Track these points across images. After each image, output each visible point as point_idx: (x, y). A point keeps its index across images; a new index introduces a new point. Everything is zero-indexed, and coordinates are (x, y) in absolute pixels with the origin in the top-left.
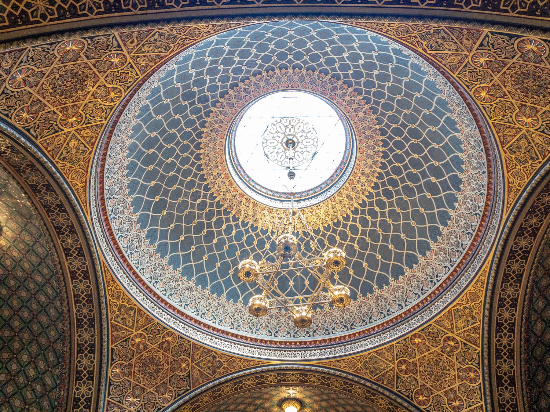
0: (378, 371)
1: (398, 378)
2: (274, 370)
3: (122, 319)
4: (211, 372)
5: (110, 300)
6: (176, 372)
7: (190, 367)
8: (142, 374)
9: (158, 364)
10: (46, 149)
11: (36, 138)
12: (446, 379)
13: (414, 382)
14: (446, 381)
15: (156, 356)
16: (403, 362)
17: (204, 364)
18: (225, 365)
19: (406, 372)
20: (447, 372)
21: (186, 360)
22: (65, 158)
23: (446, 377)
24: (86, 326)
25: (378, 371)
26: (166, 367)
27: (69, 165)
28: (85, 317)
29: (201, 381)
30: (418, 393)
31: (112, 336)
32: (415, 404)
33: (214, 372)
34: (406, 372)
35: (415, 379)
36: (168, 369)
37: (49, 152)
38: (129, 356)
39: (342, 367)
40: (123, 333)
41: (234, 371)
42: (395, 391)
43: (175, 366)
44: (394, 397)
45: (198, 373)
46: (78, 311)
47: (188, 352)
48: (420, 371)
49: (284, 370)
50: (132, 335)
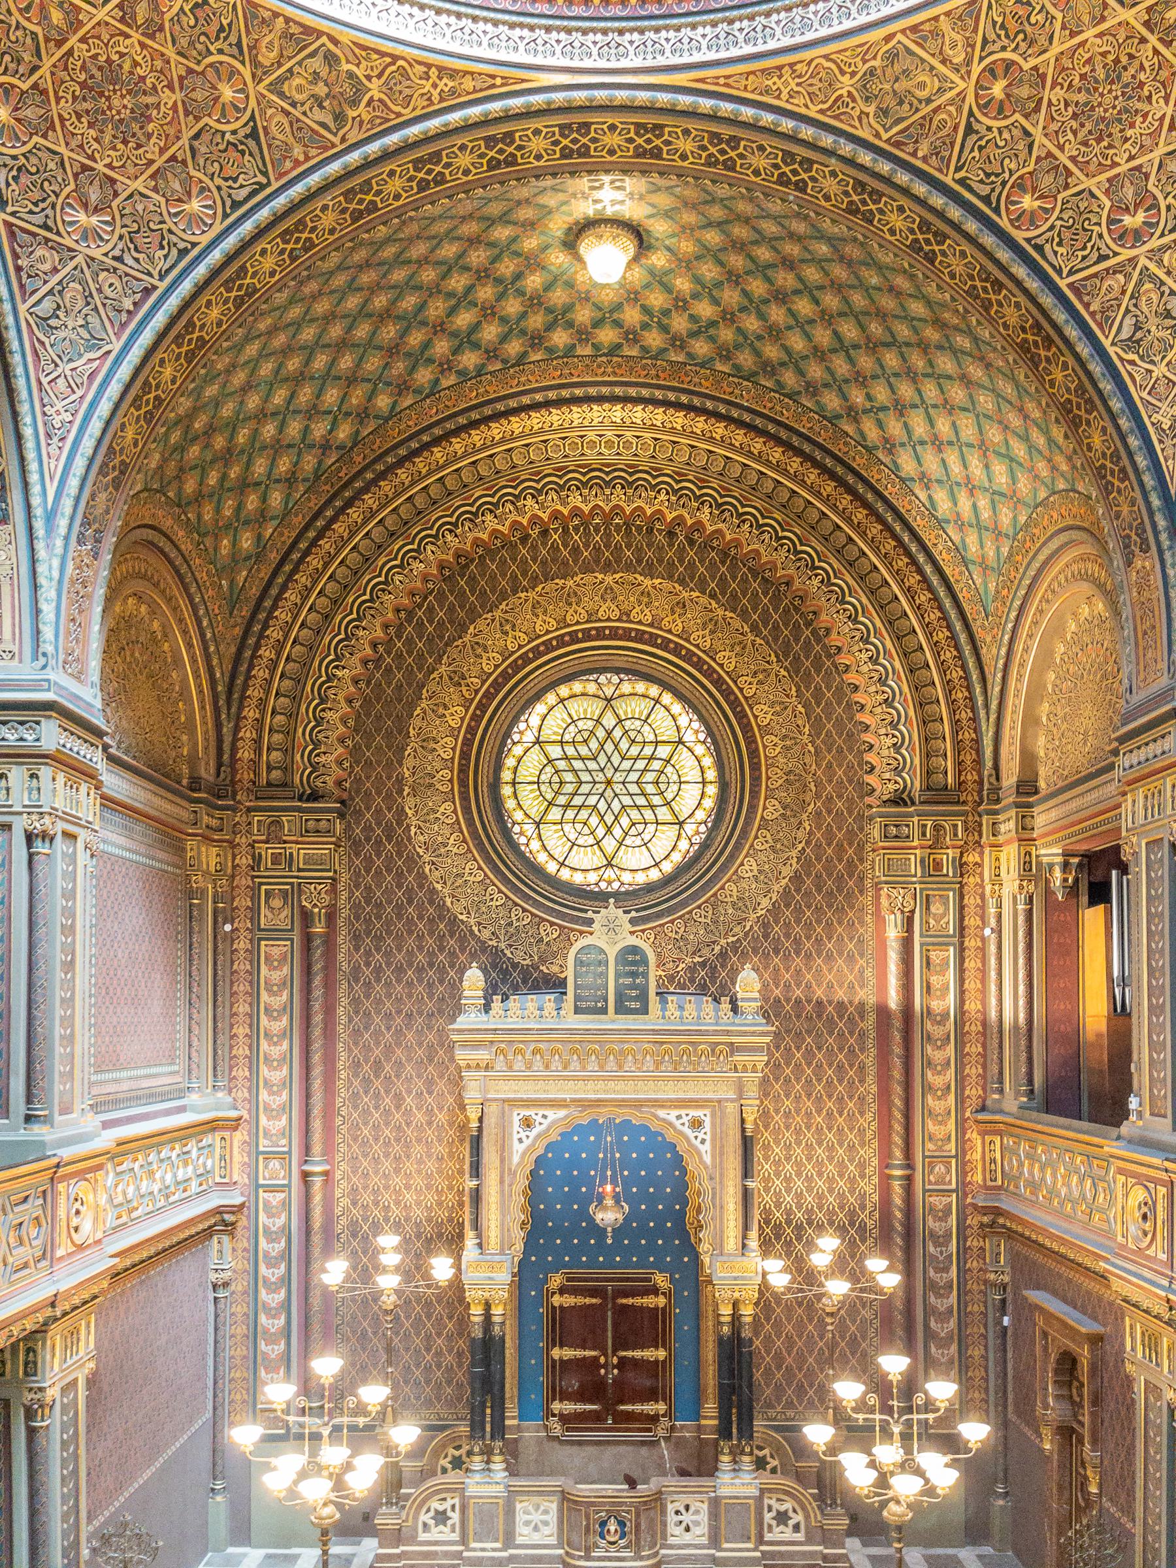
0: (906, 107)
1: (969, 130)
2: (547, 111)
4: (329, 120)
6: (206, 120)
7: (253, 103)
8: (91, 125)
9: (137, 87)
12: (1129, 133)
13: (1021, 145)
14: (1126, 140)
15: (122, 55)
16: (1000, 72)
17: (300, 88)
18: (375, 89)
19: (1001, 110)
20: (1139, 106)
21: (233, 72)
23: (1132, 125)
25: (906, 107)
26: (169, 98)
29: (298, 152)
30: (1020, 186)
32: (1004, 223)
33: (339, 117)
34: (1001, 110)
35: (1027, 133)
36: (174, 107)
38: (27, 57)
39: (784, 96)
41: (408, 114)
42: (948, 180)
43: (198, 95)
44: (938, 201)
45: (285, 121)
47: (233, 39)
48: (1050, 103)
49: (582, 109)
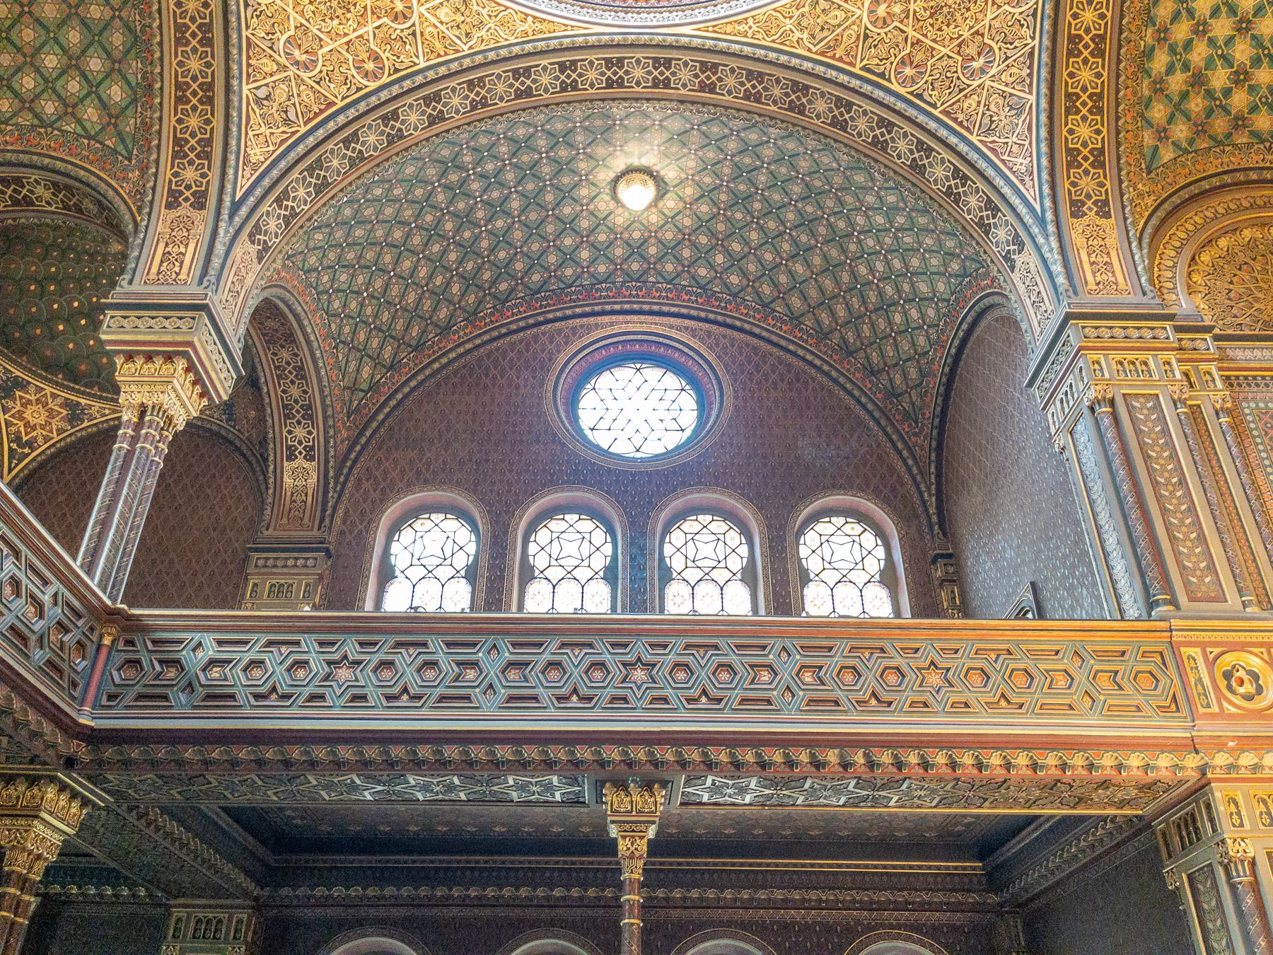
3: (823, 29)
5: (773, 41)
10: (439, 56)
11: (415, 64)
22: (467, 35)
24: (804, 100)
27: (483, 32)
28: (787, 95)
31: (840, 59)
37: (446, 54)
40: (850, 36)
46: (775, 103)
50: (865, 19)
